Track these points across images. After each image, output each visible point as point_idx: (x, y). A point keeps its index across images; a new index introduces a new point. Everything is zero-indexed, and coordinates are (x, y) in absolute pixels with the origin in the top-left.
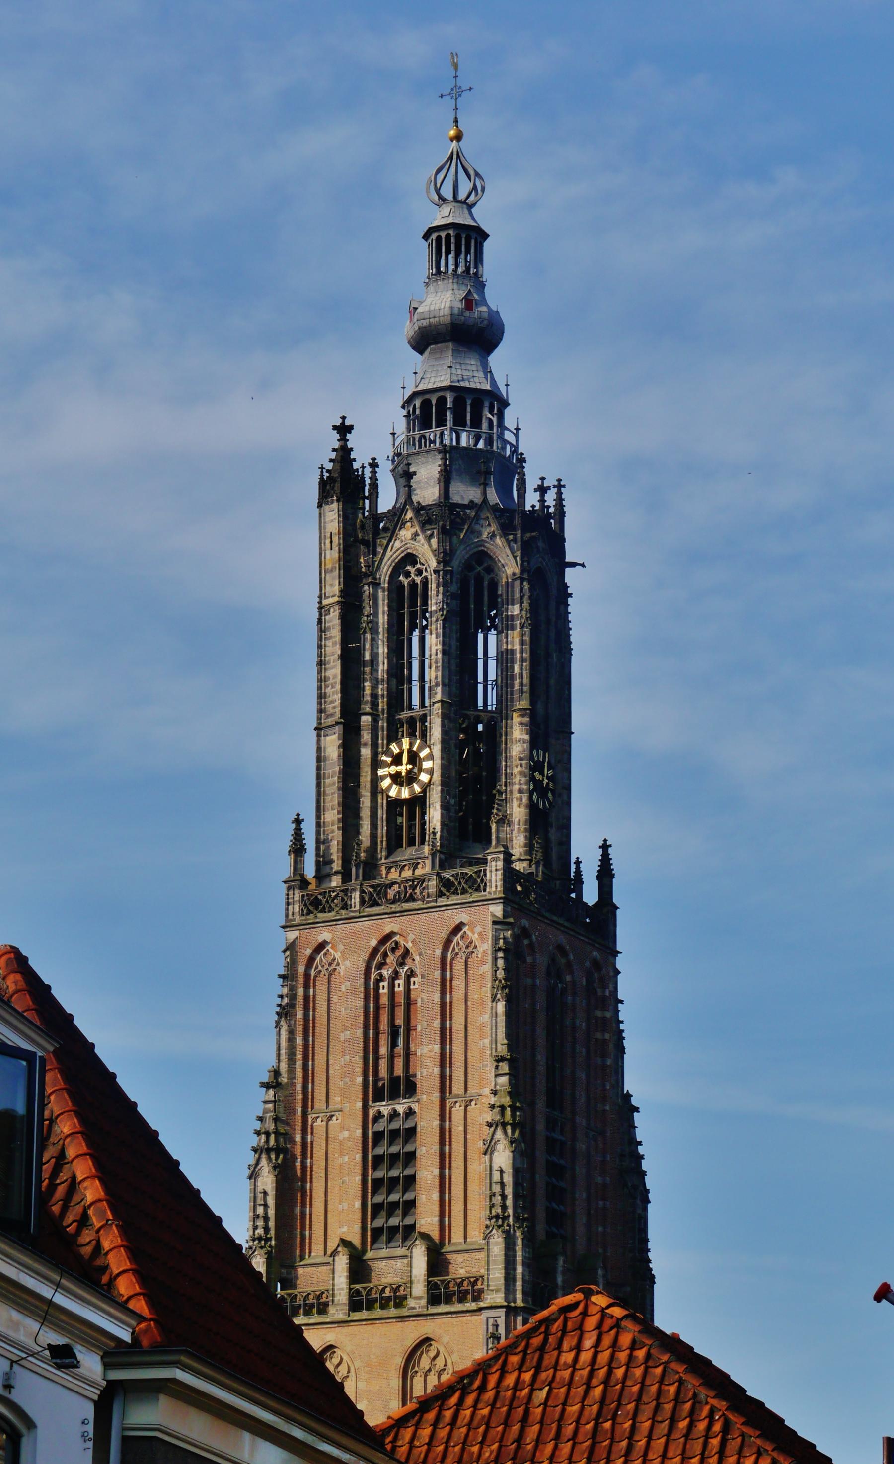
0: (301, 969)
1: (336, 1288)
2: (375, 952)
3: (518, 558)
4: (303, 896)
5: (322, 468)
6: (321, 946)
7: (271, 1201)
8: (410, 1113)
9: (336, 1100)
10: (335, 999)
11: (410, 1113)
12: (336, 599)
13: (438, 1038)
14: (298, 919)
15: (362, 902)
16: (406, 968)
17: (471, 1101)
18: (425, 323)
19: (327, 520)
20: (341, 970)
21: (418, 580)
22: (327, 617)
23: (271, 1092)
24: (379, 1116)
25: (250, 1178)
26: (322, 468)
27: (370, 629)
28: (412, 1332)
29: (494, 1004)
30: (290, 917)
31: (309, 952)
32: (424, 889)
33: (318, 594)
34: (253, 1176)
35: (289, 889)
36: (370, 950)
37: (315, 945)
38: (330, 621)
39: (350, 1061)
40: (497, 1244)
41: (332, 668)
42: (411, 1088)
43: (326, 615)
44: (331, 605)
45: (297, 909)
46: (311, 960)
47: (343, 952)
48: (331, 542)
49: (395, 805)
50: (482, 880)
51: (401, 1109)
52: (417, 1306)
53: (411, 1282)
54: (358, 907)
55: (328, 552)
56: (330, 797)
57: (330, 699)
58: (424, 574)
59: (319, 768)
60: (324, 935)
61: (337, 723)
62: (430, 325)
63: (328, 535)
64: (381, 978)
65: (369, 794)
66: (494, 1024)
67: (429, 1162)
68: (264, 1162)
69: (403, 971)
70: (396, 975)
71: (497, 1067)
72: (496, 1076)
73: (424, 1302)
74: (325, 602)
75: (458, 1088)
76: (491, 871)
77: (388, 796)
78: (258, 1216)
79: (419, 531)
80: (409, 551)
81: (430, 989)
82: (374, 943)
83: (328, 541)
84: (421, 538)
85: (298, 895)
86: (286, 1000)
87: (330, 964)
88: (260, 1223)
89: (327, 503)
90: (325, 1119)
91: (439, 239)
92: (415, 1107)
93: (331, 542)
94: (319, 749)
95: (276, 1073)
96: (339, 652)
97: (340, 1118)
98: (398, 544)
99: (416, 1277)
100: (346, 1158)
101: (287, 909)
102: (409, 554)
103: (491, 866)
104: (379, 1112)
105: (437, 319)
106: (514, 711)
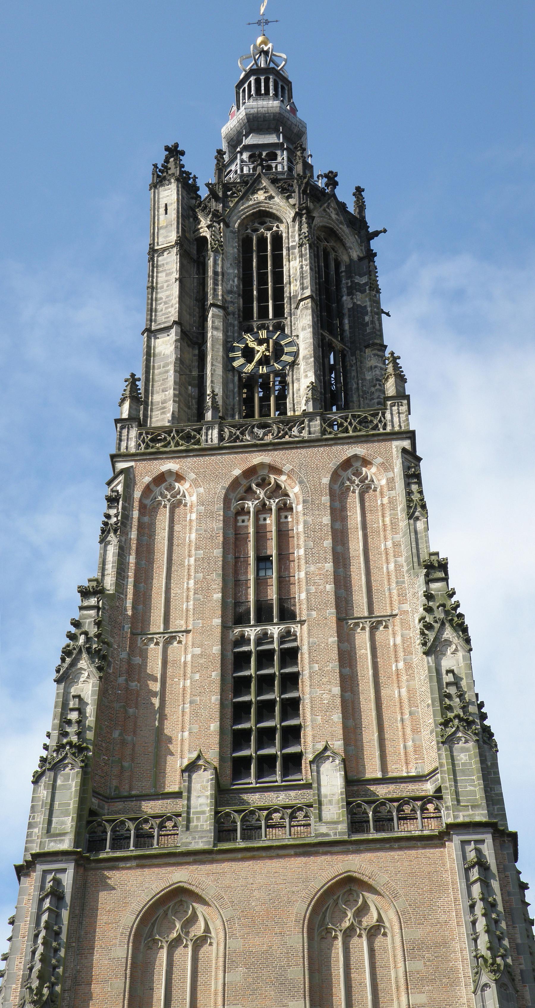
0: (137, 494)
1: (192, 811)
2: (236, 483)
3: (363, 248)
4: (141, 434)
5: (155, 166)
6: (160, 479)
7: (90, 710)
8: (286, 636)
9: (178, 623)
10: (177, 528)
11: (286, 636)
12: (173, 243)
13: (330, 557)
14: (133, 451)
15: (221, 438)
16: (277, 500)
17: (379, 623)
18: (252, 111)
19: (161, 196)
20: (192, 499)
21: (269, 235)
22: (160, 258)
23: (93, 601)
24: (243, 640)
25: (58, 681)
26: (155, 166)
27: (222, 250)
28: (325, 869)
29: (412, 521)
30: (123, 449)
31: (147, 479)
32: (303, 428)
33: (149, 241)
34: (65, 677)
35: (122, 428)
36: (231, 479)
37: (156, 473)
38: (164, 260)
39: (204, 577)
40: (463, 750)
41: (166, 291)
42: (287, 614)
43: (158, 256)
44: (164, 250)
45: (132, 444)
46: (148, 490)
47: (194, 481)
48: (166, 210)
49: (249, 383)
50: (380, 421)
51: (275, 630)
52: (331, 833)
53: (320, 803)
54: (216, 441)
55: (162, 217)
56: (160, 383)
57: (163, 312)
58: (275, 229)
59: (148, 361)
60: (171, 465)
61: (175, 322)
62: (258, 113)
63: (162, 206)
64: (242, 511)
65: (221, 366)
66: (413, 539)
67: (325, 680)
68: (84, 663)
69: (273, 504)
70: (263, 509)
71: (427, 575)
72: (427, 583)
73: (343, 827)
74: (156, 248)
75: (360, 606)
76: (392, 414)
77: (240, 373)
78: (69, 722)
79: (273, 194)
80: (261, 208)
81: (317, 512)
82: (237, 472)
83: (162, 210)
84: (278, 200)
85: (134, 432)
86: (114, 520)
87: (173, 496)
88: (72, 730)
89: (162, 185)
90: (161, 641)
91: (258, 81)
92: (295, 628)
93: (166, 210)
94: (149, 347)
95: (99, 582)
96: (178, 276)
97: (183, 639)
98: (251, 203)
99: (326, 796)
100: (197, 676)
101: (120, 444)
102: (260, 210)
103: (391, 410)
104: (243, 636)
105: (266, 109)
106: (367, 346)
